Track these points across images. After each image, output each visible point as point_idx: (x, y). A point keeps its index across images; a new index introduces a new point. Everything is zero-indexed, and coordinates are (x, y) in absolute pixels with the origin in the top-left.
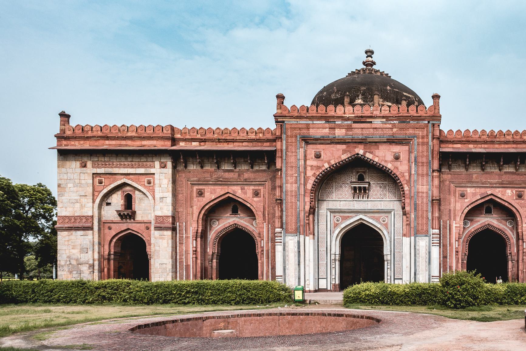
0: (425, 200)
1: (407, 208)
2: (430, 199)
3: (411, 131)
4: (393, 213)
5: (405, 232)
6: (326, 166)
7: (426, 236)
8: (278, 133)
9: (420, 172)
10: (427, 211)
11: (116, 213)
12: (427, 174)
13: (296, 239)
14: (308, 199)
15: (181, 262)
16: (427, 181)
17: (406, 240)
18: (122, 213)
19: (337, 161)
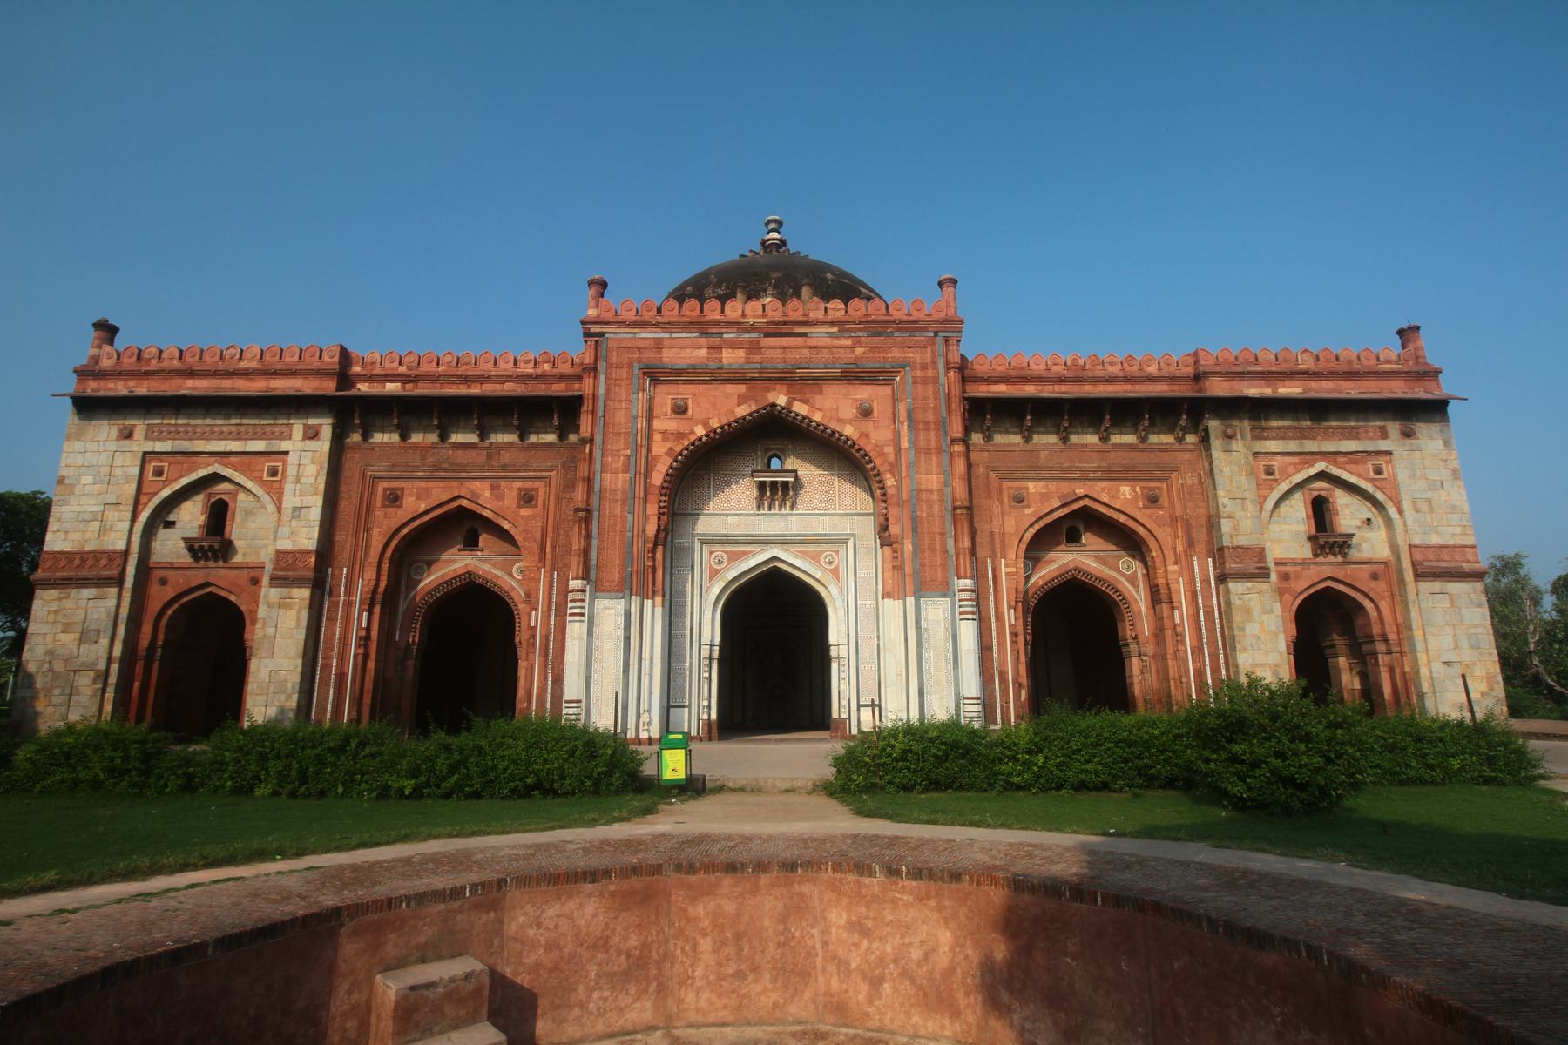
0: (936, 509)
1: (894, 529)
2: (949, 505)
3: (896, 354)
4: (850, 544)
5: (889, 588)
6: (700, 431)
7: (944, 596)
8: (588, 360)
9: (922, 444)
10: (942, 534)
11: (182, 544)
12: (939, 450)
13: (620, 605)
14: (652, 509)
15: (327, 666)
16: (940, 464)
17: (892, 607)
18: (197, 545)
19: (725, 421)
